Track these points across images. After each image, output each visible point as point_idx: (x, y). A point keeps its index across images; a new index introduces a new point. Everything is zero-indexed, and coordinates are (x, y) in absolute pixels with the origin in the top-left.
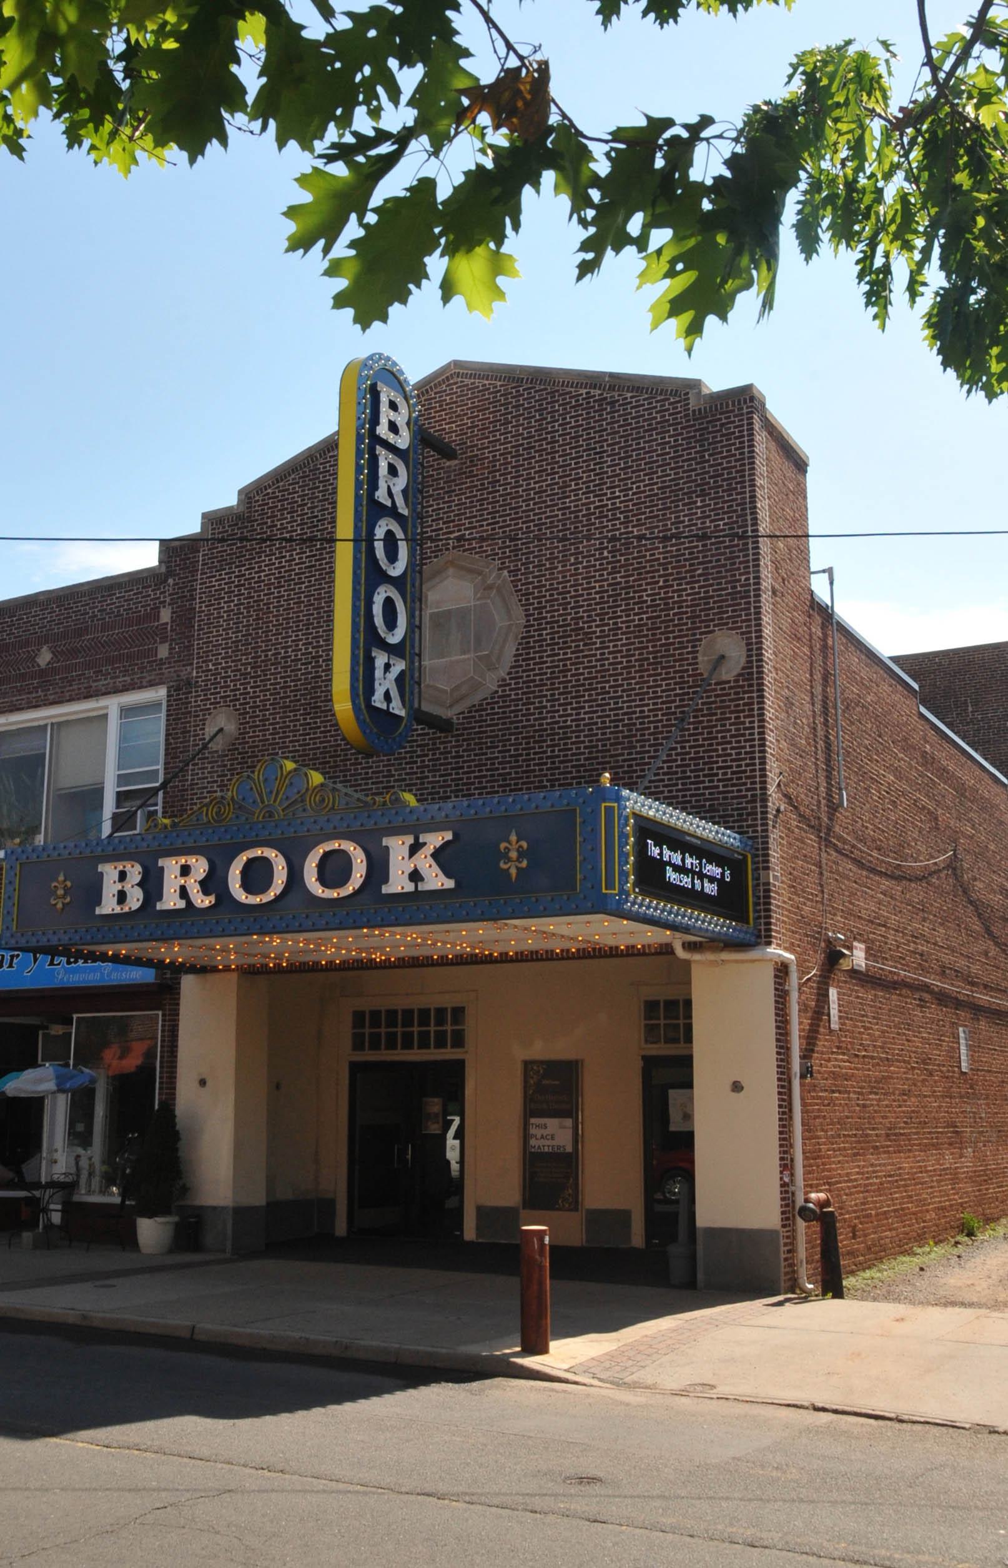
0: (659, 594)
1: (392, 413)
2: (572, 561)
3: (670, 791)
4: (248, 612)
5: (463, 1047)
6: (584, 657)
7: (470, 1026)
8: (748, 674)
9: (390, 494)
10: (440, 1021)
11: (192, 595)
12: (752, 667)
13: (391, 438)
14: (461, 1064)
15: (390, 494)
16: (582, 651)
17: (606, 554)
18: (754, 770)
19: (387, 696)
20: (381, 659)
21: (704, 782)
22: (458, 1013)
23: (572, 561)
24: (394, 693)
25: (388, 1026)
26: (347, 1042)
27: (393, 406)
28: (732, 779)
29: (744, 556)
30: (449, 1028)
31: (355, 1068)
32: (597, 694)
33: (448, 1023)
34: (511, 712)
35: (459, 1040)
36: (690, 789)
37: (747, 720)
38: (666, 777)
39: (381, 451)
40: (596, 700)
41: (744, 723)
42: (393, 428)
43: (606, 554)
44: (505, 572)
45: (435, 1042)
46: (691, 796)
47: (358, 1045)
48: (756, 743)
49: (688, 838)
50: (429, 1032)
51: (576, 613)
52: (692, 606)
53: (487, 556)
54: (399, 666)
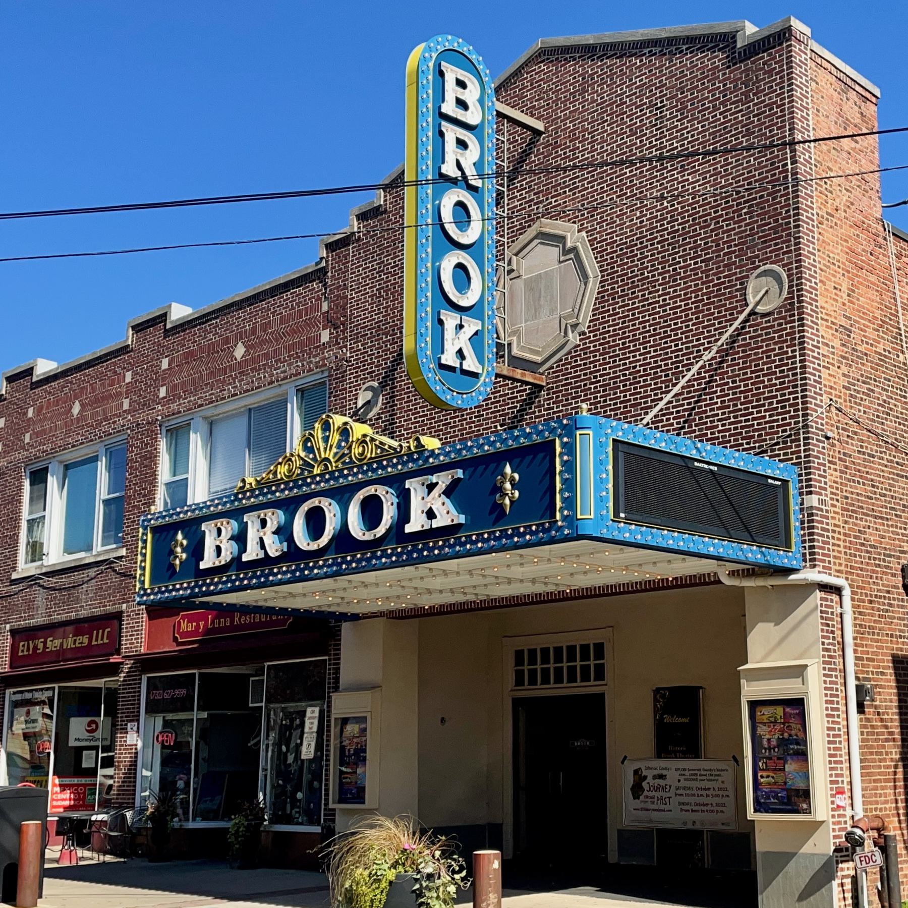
0: (711, 236)
1: (460, 90)
2: (638, 214)
3: (723, 425)
4: (387, 295)
5: (604, 680)
6: (649, 304)
7: (609, 662)
8: (790, 304)
9: (459, 166)
10: (585, 656)
11: (345, 285)
12: (793, 298)
13: (459, 114)
14: (602, 696)
15: (459, 166)
16: (647, 299)
17: (666, 204)
18: (797, 398)
19: (460, 354)
20: (451, 320)
21: (752, 413)
22: (599, 649)
23: (638, 214)
24: (468, 352)
25: (542, 663)
26: (511, 678)
27: (461, 84)
28: (777, 408)
29: (785, 189)
30: (592, 663)
31: (517, 703)
32: (661, 339)
33: (591, 658)
34: (590, 363)
35: (600, 674)
36: (741, 422)
37: (789, 350)
38: (720, 412)
39: (446, 126)
40: (660, 344)
41: (787, 352)
42: (462, 104)
43: (666, 204)
44: (584, 234)
45: (581, 677)
46: (742, 427)
47: (519, 681)
48: (798, 371)
49: (696, 464)
50: (576, 666)
51: (642, 264)
52: (739, 244)
53: (569, 220)
54: (472, 326)
